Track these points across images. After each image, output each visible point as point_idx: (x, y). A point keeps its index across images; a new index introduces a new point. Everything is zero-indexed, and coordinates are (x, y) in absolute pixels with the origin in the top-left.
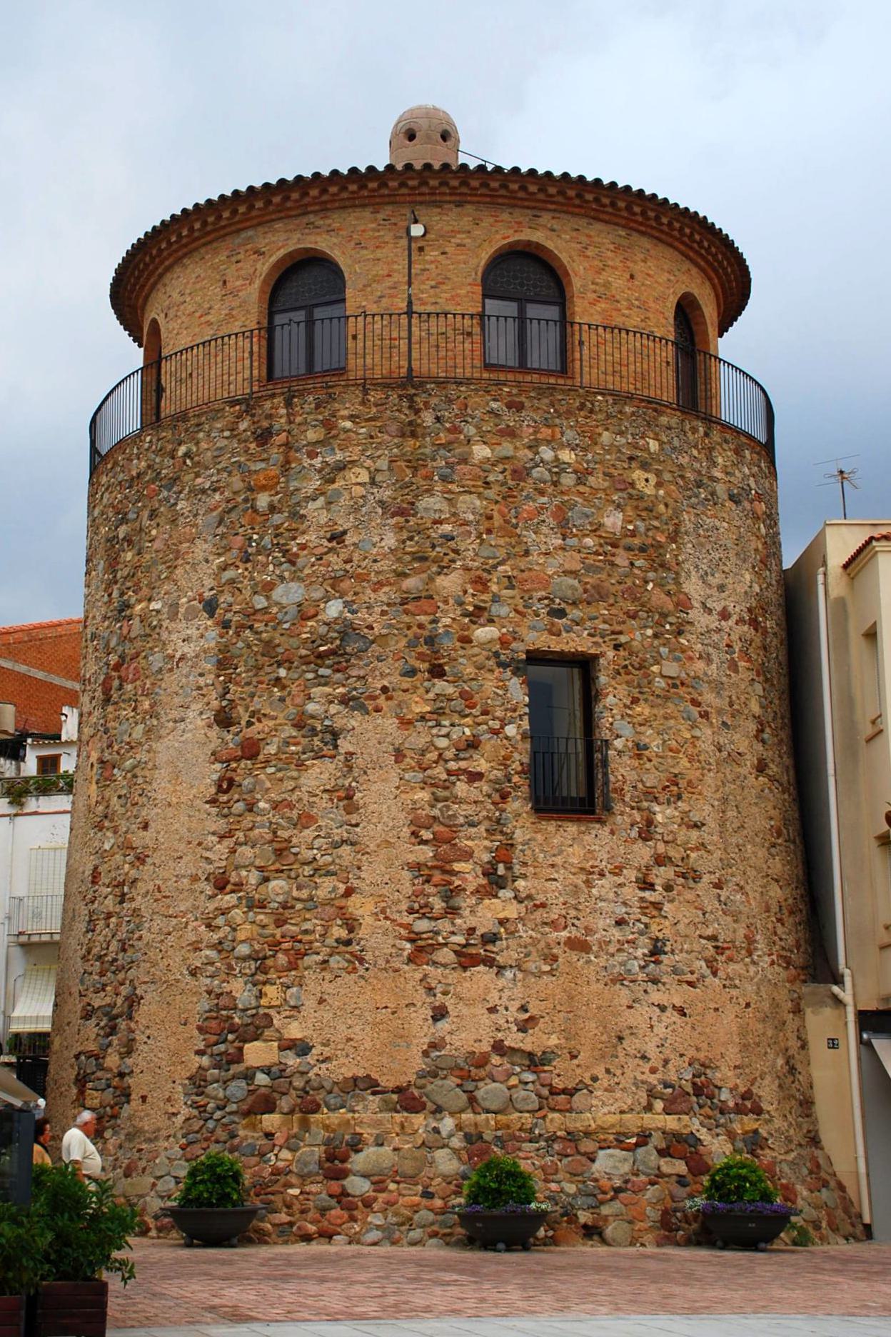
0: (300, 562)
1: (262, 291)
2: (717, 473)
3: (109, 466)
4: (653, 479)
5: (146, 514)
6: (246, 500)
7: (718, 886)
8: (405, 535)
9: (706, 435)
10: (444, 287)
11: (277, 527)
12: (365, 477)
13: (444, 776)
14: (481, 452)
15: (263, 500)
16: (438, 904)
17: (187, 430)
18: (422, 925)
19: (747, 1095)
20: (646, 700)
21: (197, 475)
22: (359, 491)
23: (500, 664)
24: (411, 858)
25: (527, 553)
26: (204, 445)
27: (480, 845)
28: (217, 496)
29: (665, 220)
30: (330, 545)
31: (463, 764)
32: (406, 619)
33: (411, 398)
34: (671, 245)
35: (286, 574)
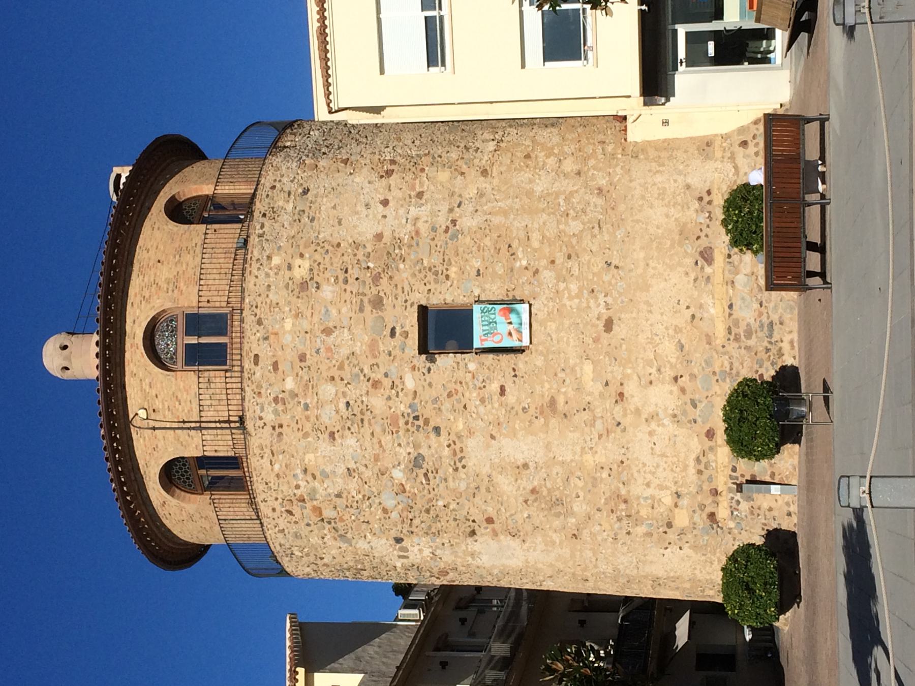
4: (298, 261)
6: (329, 523)
8: (347, 432)
10: (179, 397)
20: (447, 269)
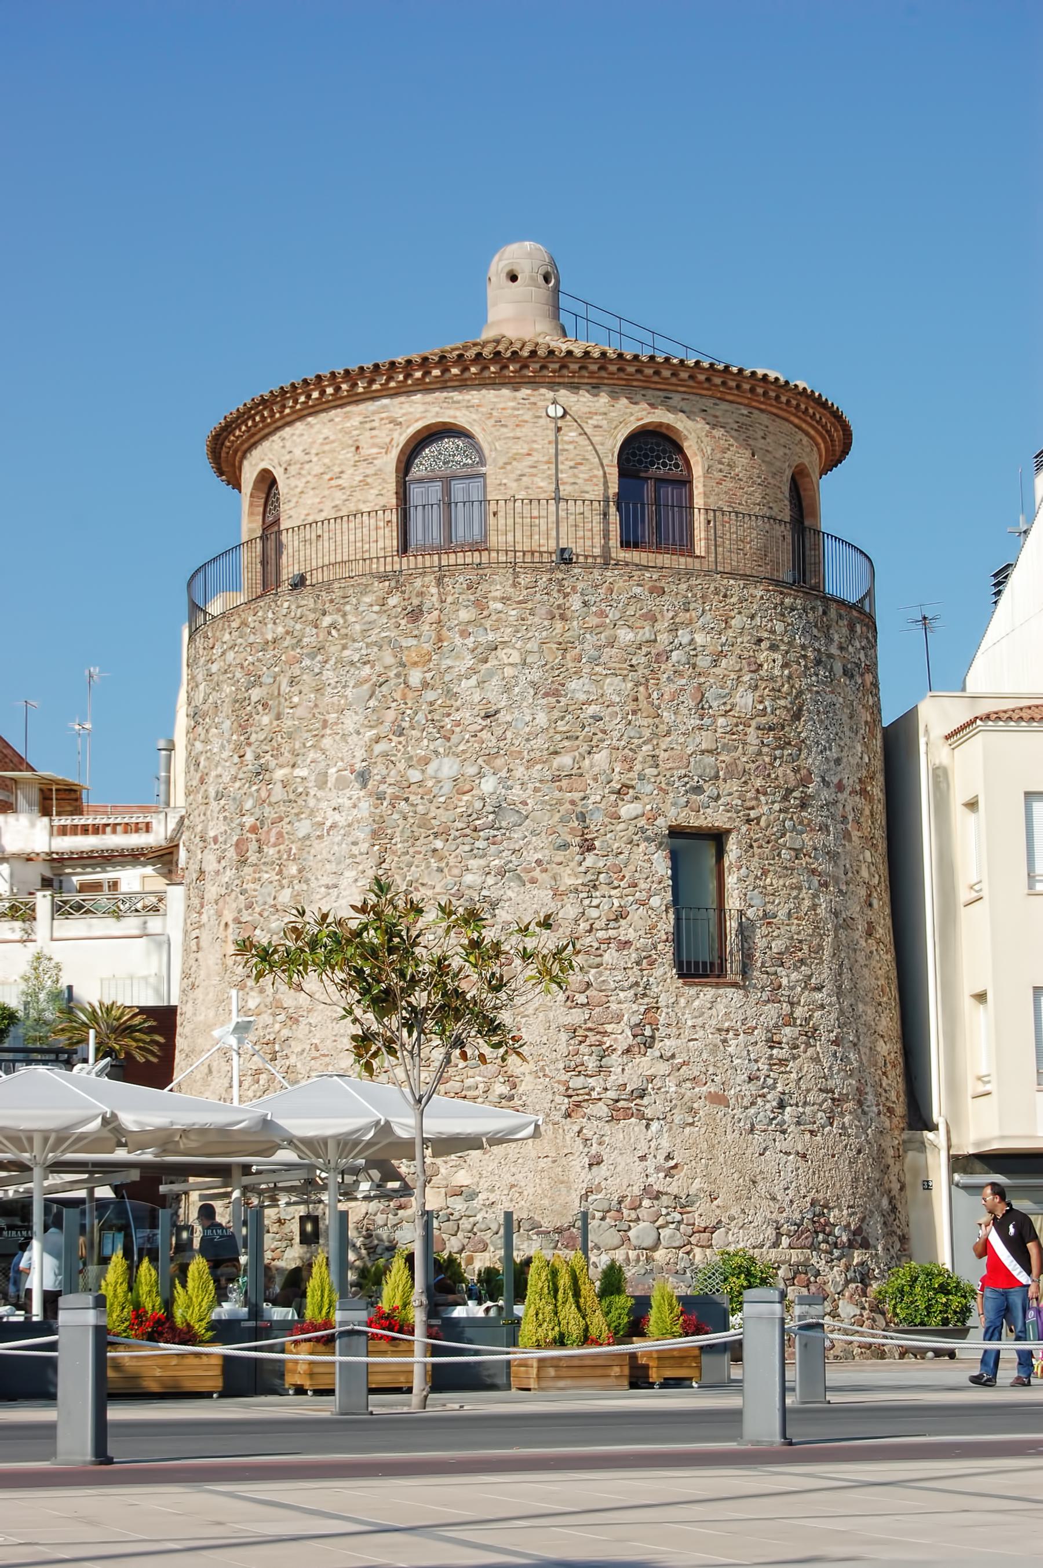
0: (455, 739)
1: (399, 461)
2: (834, 650)
3: (234, 625)
5: (284, 681)
6: (398, 675)
7: (836, 1042)
8: (556, 714)
9: (825, 613)
10: (582, 468)
11: (431, 704)
12: (516, 658)
13: (596, 945)
14: (625, 636)
15: (415, 677)
16: (591, 1063)
17: (332, 601)
18: (577, 1082)
19: (858, 1232)
21: (344, 647)
22: (509, 671)
23: (647, 839)
24: (568, 1020)
25: (668, 733)
26: (351, 618)
27: (631, 1011)
28: (367, 670)
29: (784, 399)
30: (484, 723)
31: (611, 933)
32: (557, 794)
33: (560, 582)
34: (787, 420)
35: (441, 750)
